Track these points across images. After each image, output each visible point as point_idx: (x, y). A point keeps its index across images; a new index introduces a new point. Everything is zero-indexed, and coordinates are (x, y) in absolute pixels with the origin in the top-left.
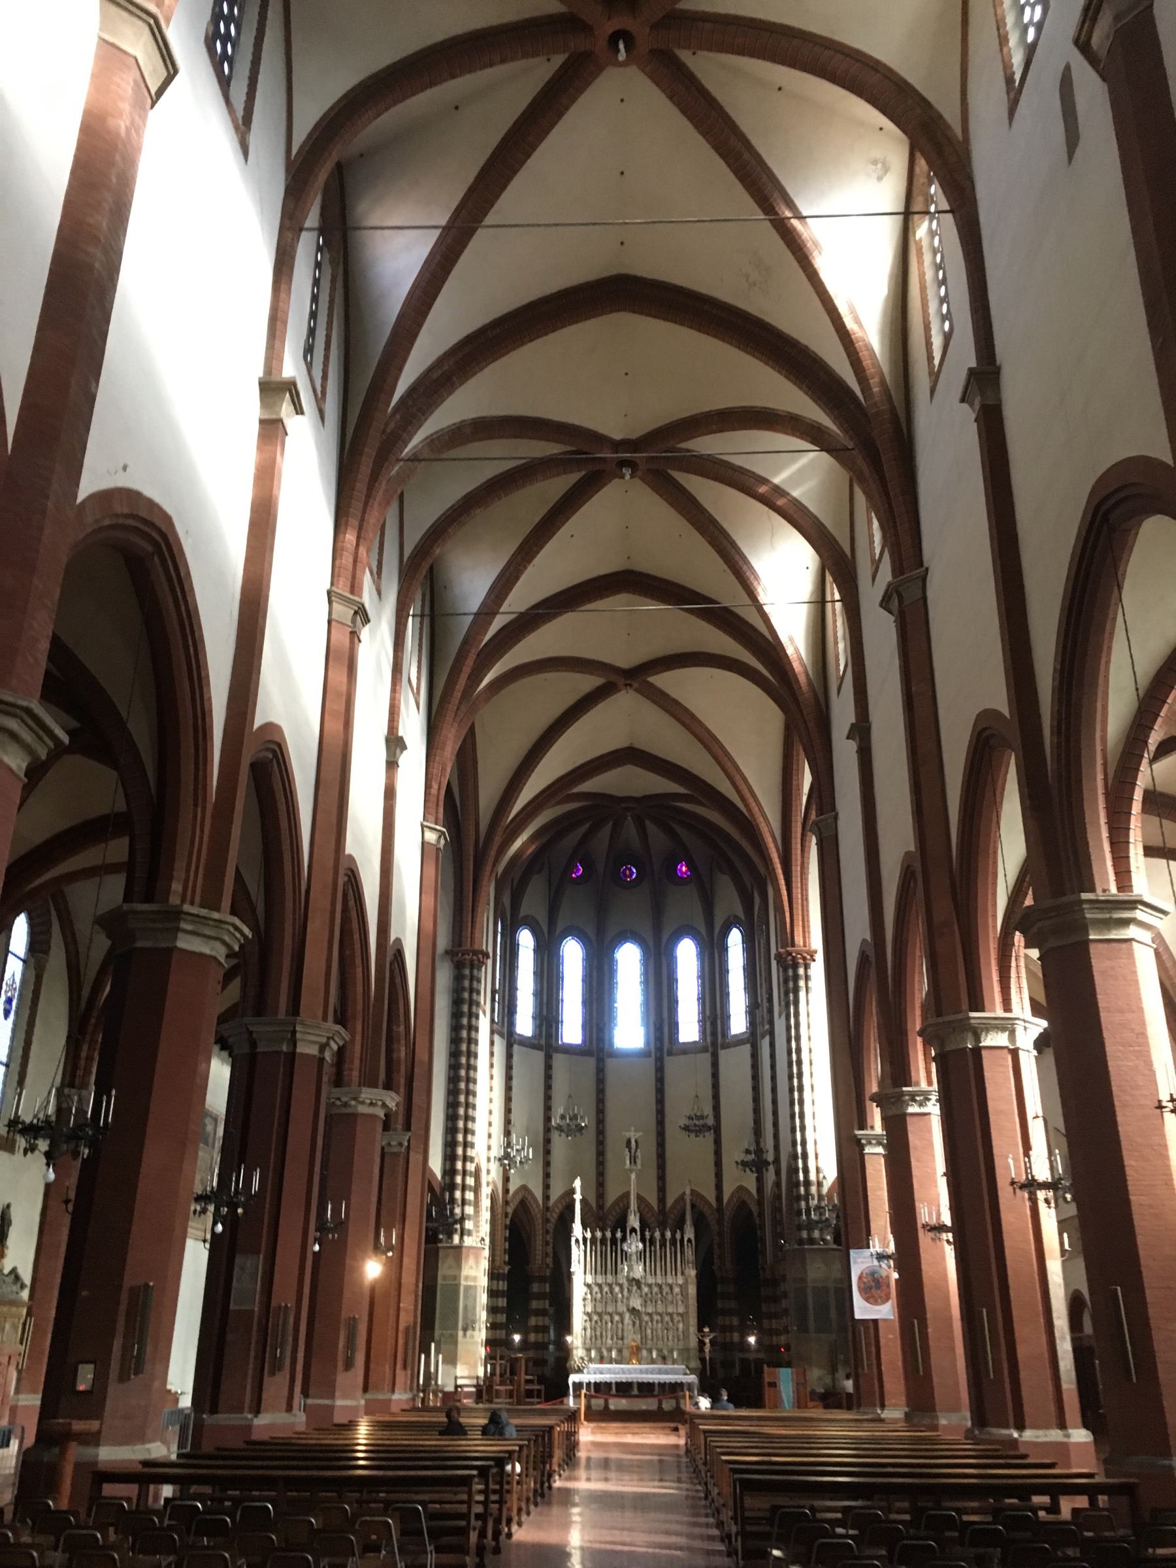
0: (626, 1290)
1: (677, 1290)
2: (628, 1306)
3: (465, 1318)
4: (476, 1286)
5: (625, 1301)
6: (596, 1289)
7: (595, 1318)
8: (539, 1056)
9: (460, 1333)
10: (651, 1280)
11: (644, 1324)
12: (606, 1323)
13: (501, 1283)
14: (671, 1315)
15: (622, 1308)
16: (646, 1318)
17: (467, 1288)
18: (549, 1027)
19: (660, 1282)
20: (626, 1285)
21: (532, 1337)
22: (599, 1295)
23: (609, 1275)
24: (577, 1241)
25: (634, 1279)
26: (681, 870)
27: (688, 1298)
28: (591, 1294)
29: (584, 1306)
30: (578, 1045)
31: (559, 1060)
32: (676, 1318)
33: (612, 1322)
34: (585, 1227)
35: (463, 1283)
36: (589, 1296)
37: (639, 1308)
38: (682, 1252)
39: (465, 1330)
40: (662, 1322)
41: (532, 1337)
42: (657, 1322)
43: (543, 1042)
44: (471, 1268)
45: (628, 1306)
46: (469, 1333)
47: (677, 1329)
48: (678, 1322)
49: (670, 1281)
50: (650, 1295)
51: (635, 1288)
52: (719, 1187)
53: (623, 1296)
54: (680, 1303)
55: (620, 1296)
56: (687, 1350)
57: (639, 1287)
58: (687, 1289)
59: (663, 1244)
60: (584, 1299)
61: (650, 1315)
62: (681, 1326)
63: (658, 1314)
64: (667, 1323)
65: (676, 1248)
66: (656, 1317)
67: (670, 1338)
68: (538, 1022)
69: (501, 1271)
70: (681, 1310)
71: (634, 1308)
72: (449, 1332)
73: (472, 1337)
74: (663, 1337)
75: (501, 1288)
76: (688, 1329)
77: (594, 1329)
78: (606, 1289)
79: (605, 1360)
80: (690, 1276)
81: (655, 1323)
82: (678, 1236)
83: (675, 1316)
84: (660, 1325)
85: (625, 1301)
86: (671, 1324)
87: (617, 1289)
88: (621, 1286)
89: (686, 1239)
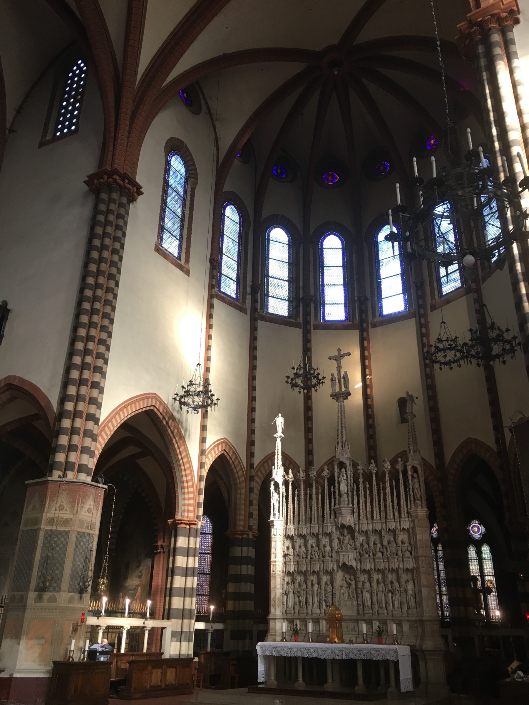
0: (336, 541)
1: (402, 537)
2: (338, 561)
3: (42, 577)
4: (67, 533)
5: (334, 555)
6: (299, 542)
7: (299, 579)
8: (297, 334)
9: (32, 595)
10: (366, 526)
11: (360, 585)
12: (312, 585)
13: (192, 539)
14: (396, 571)
15: (331, 566)
16: (363, 578)
17: (50, 535)
18: (307, 306)
19: (378, 527)
20: (336, 534)
21: (230, 605)
22: (303, 549)
23: (315, 524)
24: (277, 485)
25: (343, 526)
26: (430, 144)
27: (416, 547)
28: (293, 548)
29: (285, 563)
30: (341, 321)
31: (317, 336)
32: (404, 577)
33: (319, 584)
34: (286, 471)
35: (44, 526)
36: (291, 550)
37: (354, 565)
38: (406, 487)
39: (41, 590)
40: (384, 582)
41: (230, 605)
42: (378, 582)
43: (301, 320)
44: (61, 508)
45: (338, 561)
46: (46, 596)
47: (406, 591)
48: (407, 581)
49: (392, 526)
50: (366, 546)
51: (348, 537)
52: (498, 427)
53: (331, 548)
54: (407, 554)
55: (328, 548)
56: (421, 622)
57: (353, 538)
58: (415, 534)
59: (381, 478)
60: (285, 556)
61: (368, 572)
62: (410, 586)
63: (378, 571)
64: (392, 582)
65: (398, 482)
66: (375, 576)
67: (396, 604)
68: (295, 304)
69: (245, 536)
70: (410, 564)
71: (344, 564)
72: (20, 593)
73: (53, 600)
74: (386, 603)
75: (192, 545)
76: (420, 591)
77: (298, 594)
78: (311, 541)
79: (300, 638)
80: (417, 516)
81: (375, 583)
82: (400, 466)
83: (401, 572)
84: (382, 586)
85: (334, 555)
86: (396, 585)
87: (325, 540)
88: (329, 535)
89: (409, 468)
